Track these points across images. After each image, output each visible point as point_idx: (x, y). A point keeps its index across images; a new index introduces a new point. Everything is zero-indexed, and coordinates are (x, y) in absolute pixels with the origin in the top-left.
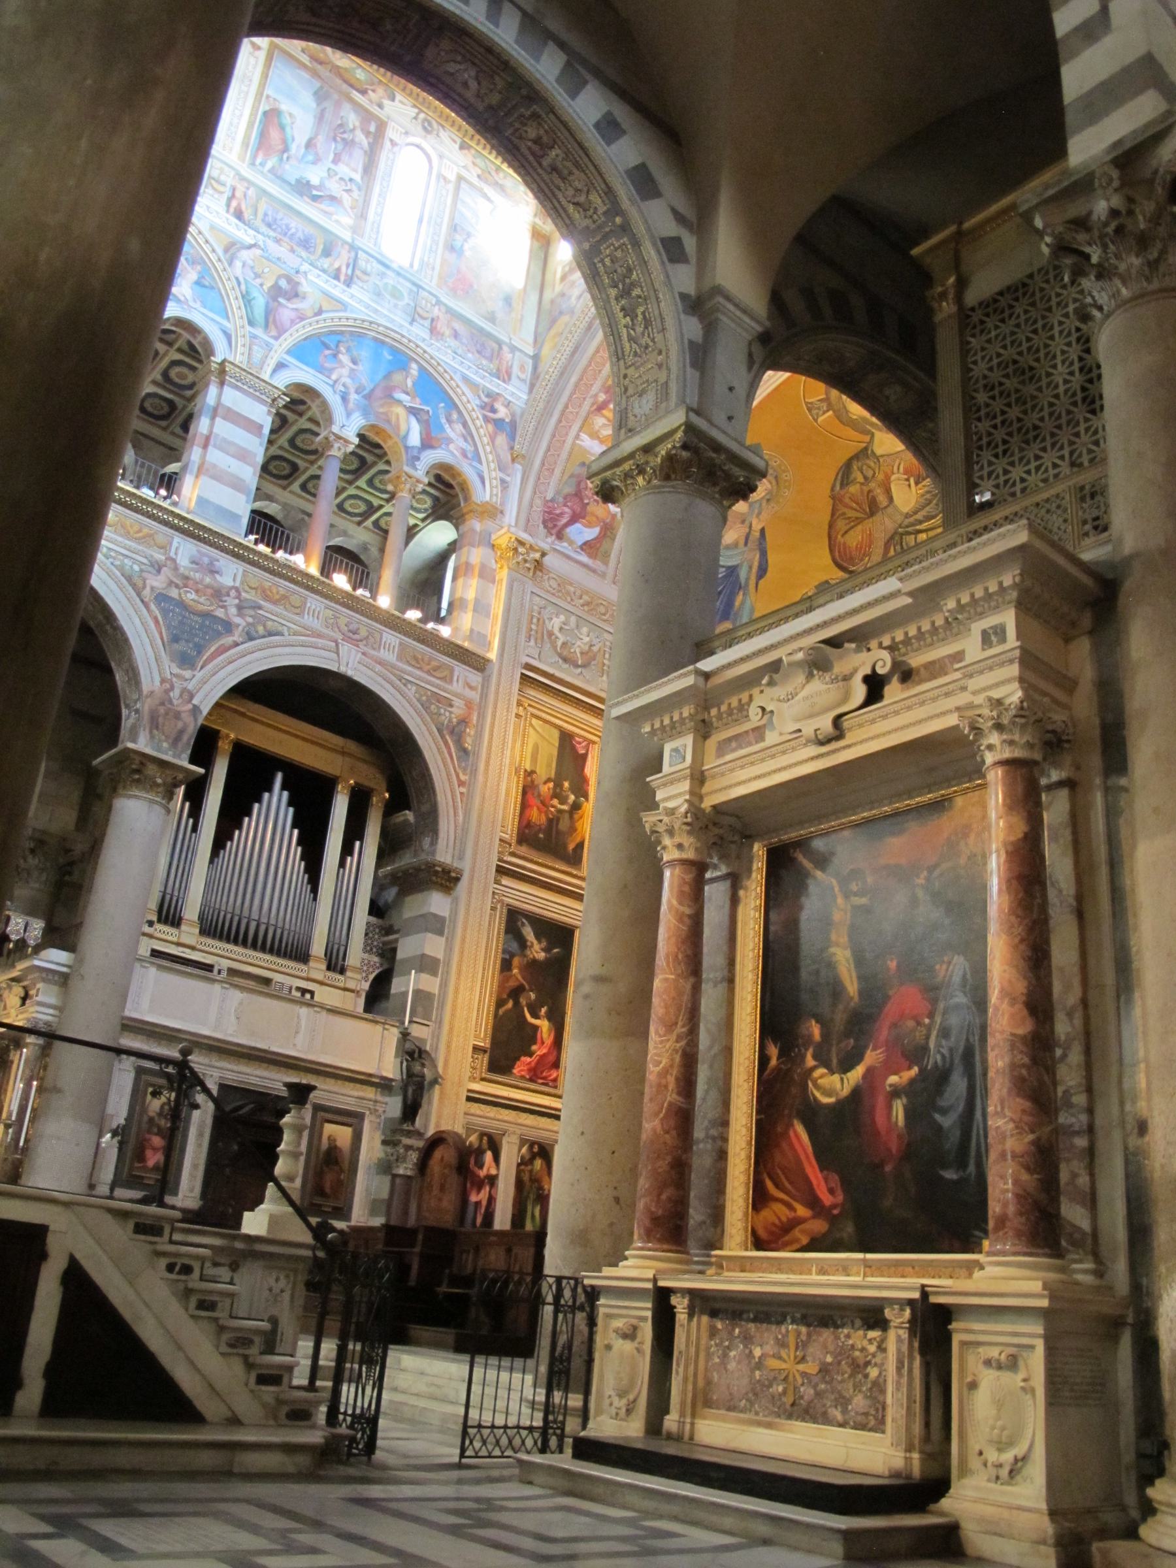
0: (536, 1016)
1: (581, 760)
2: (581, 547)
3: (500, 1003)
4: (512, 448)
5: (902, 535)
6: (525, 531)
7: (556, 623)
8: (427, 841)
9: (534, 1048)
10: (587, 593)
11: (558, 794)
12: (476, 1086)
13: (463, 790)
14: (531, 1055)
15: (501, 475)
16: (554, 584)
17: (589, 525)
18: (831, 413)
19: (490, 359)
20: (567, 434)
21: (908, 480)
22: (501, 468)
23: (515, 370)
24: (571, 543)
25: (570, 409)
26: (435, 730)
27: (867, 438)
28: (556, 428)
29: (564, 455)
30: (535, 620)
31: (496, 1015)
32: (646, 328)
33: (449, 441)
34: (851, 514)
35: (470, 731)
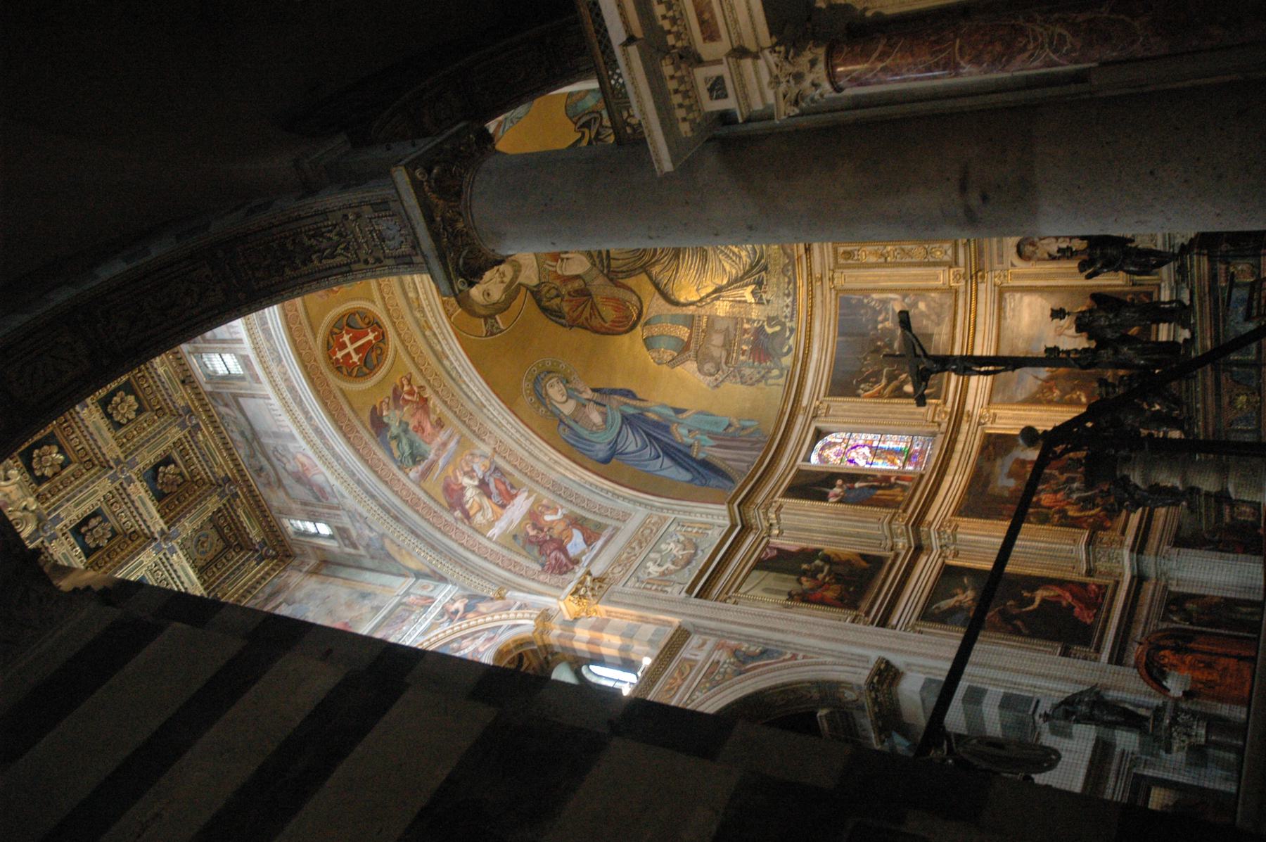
0: (1032, 601)
1: (783, 554)
2: (589, 545)
3: (1017, 632)
4: (492, 599)
5: (609, 271)
6: (563, 589)
7: (653, 569)
8: (850, 695)
9: (1064, 603)
10: (630, 543)
11: (813, 574)
12: (1105, 656)
13: (801, 655)
14: (1071, 608)
15: (513, 610)
16: (618, 569)
17: (570, 537)
18: (497, 317)
19: (412, 612)
20: (486, 547)
21: (562, 260)
22: (508, 608)
23: (425, 593)
24: (583, 553)
25: (464, 542)
26: (739, 678)
27: (523, 290)
28: (479, 556)
29: (505, 552)
30: (649, 586)
31: (1028, 636)
32: (322, 235)
33: (476, 650)
34: (587, 313)
35: (745, 646)
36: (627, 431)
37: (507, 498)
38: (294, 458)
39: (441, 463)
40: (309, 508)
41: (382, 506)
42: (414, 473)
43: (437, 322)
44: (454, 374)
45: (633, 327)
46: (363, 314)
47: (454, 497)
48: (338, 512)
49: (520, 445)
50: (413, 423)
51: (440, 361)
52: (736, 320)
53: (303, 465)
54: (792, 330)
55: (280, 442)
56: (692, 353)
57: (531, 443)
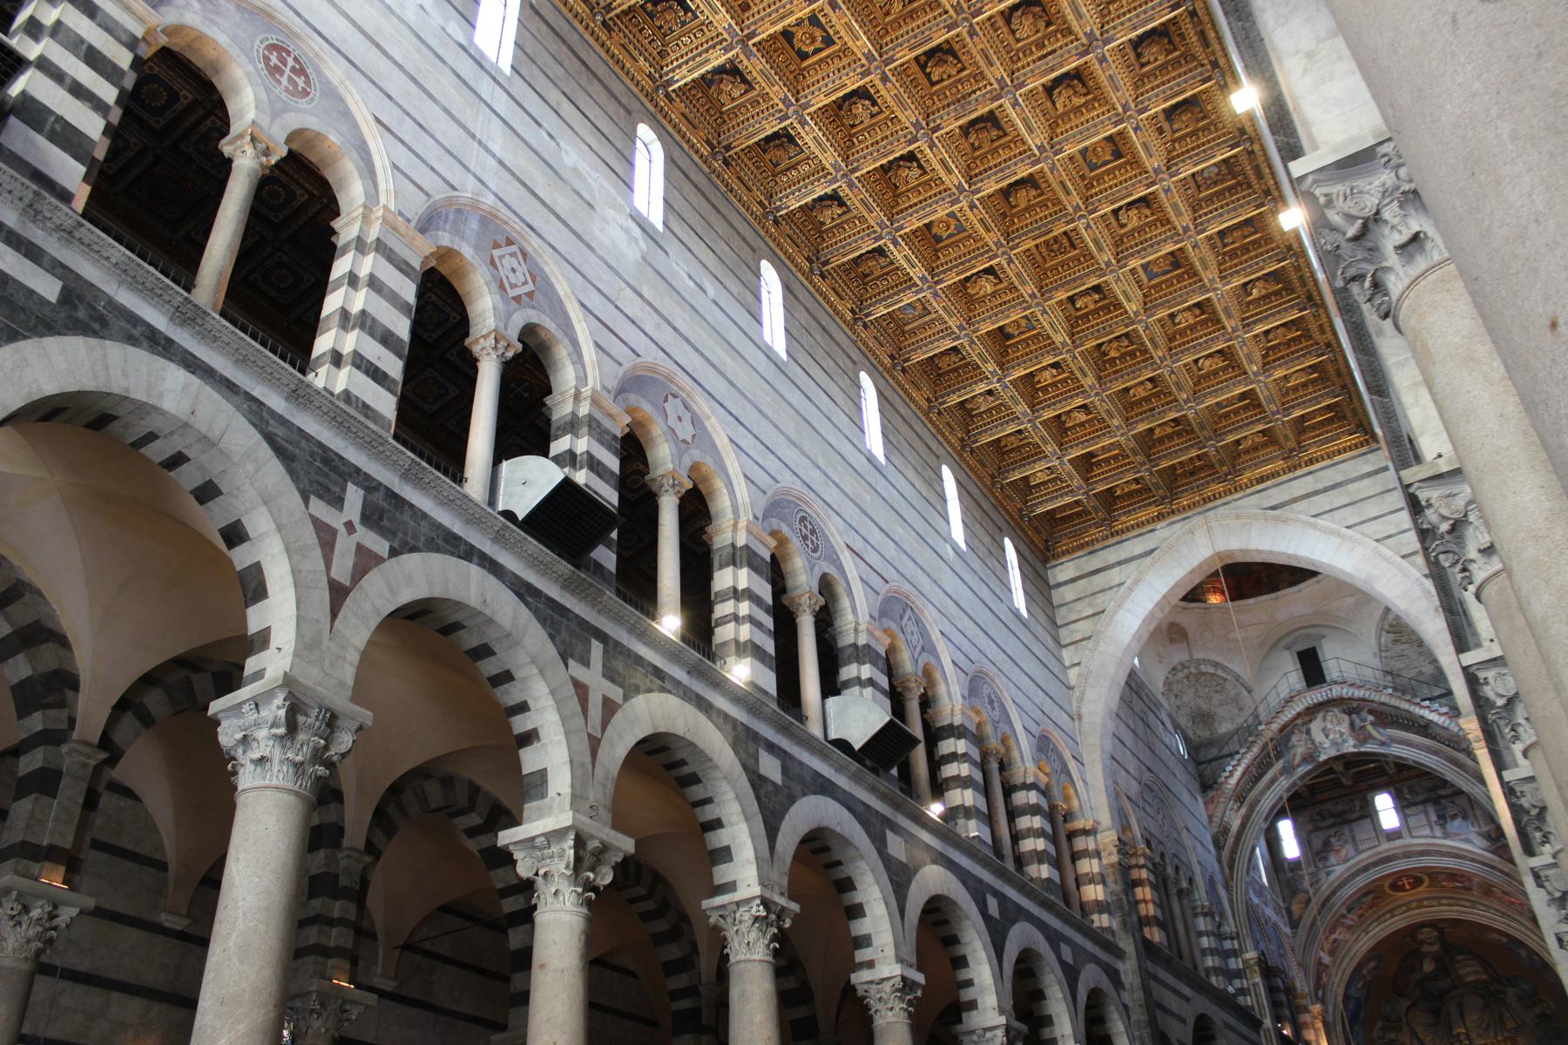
37: (1332, 953)
38: (1342, 846)
41: (1328, 899)
42: (1344, 912)
47: (1332, 931)
51: (1388, 912)
53: (1339, 851)
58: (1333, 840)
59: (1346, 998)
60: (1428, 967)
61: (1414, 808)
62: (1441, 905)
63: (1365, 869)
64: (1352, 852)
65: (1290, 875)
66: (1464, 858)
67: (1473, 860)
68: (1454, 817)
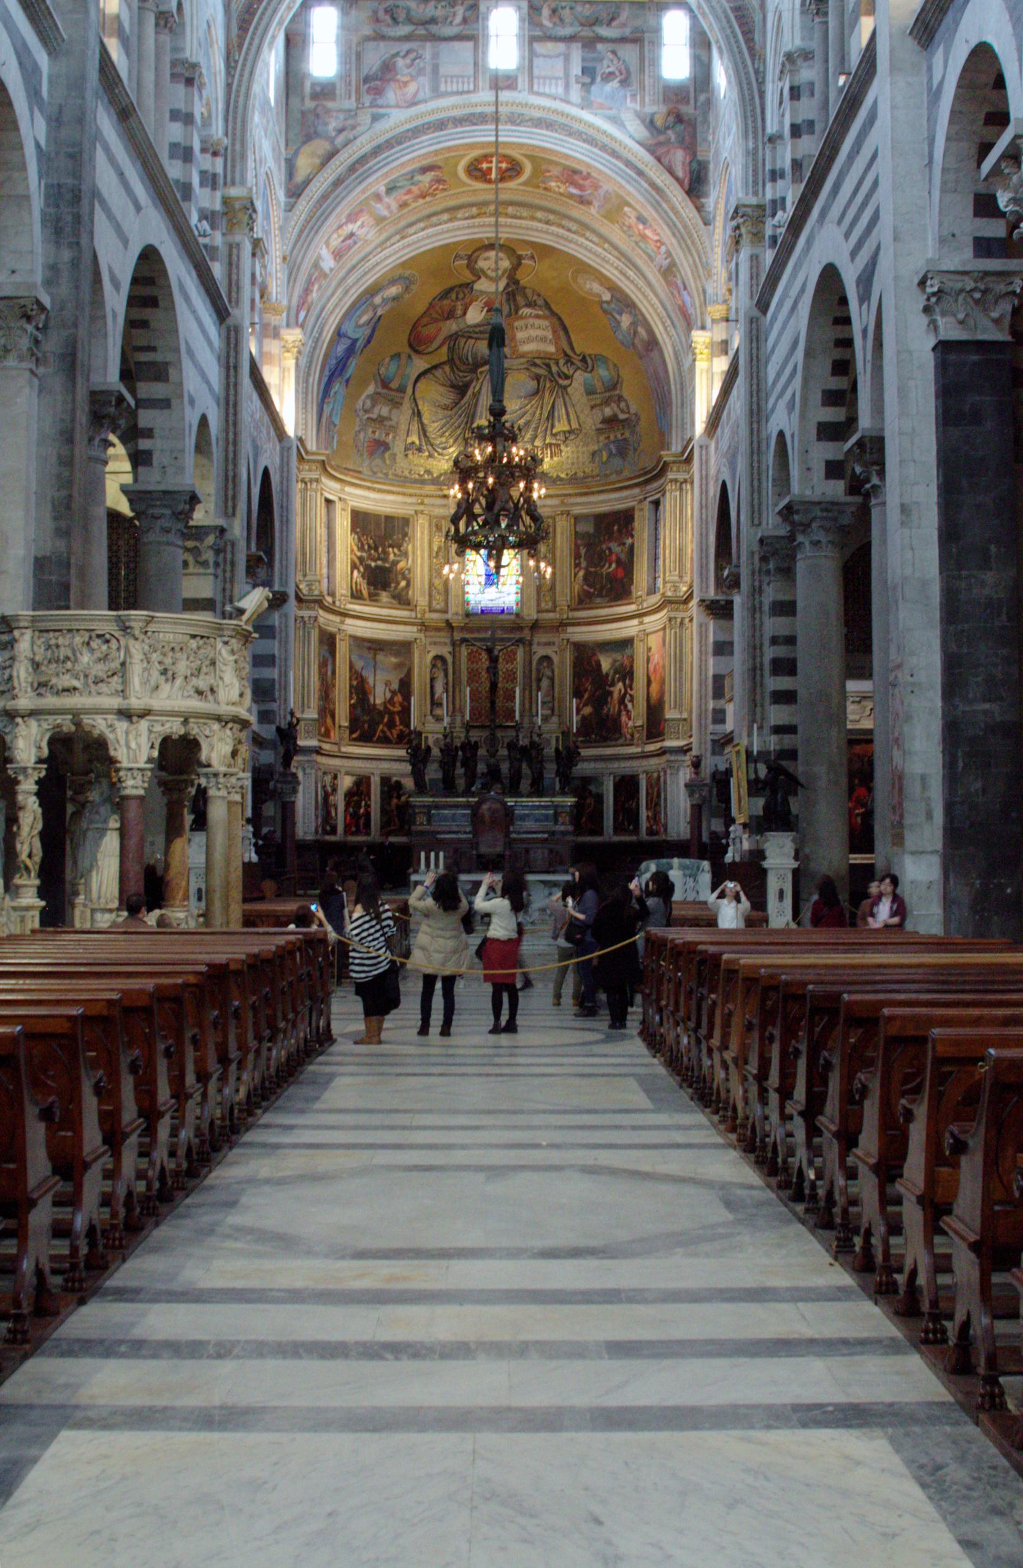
34: (435, 316)
36: (349, 342)
37: (338, 255)
38: (413, 78)
39: (379, 206)
40: (354, 58)
41: (363, 160)
42: (382, 189)
43: (483, 226)
44: (434, 219)
45: (411, 346)
46: (511, 178)
47: (352, 218)
48: (353, 98)
49: (363, 259)
50: (415, 189)
52: (394, 429)
53: (406, 84)
54: (386, 475)
55: (429, 69)
56: (380, 390)
57: (366, 273)
58: (400, 63)
59: (339, 334)
60: (475, 315)
61: (549, 47)
62: (533, 218)
63: (441, 125)
64: (426, 92)
65: (309, 104)
66: (604, 148)
67: (614, 154)
68: (609, 77)
